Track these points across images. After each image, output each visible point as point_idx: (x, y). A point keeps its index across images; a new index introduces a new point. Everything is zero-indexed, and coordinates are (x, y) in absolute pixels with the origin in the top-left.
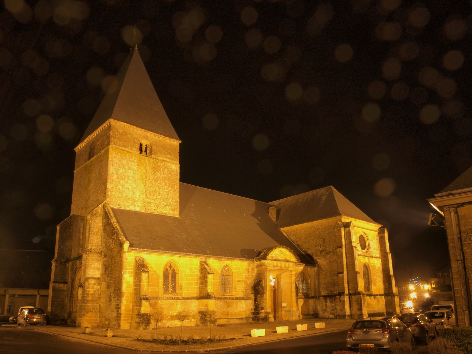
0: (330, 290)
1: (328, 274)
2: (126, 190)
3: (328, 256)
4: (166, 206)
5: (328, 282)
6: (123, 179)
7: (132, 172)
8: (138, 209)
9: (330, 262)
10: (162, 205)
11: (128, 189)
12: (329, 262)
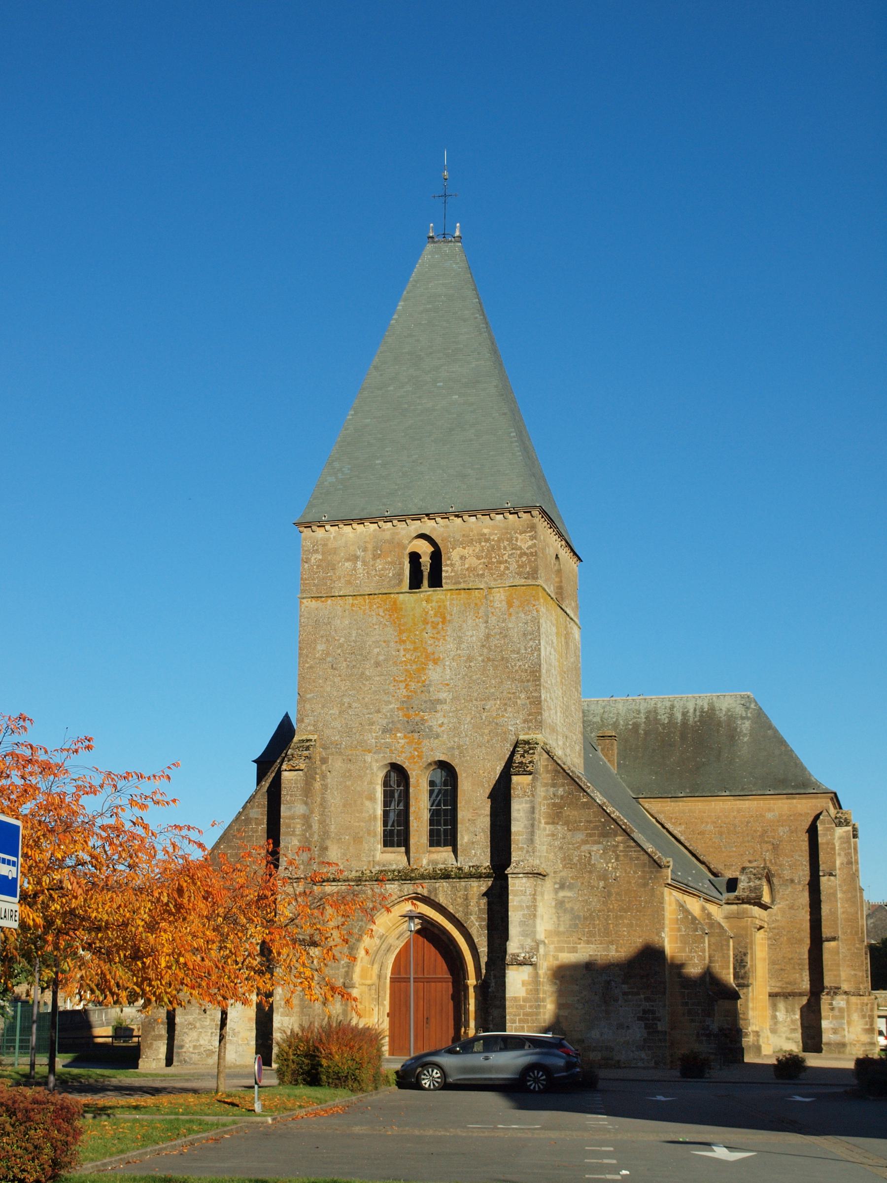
0: (787, 980)
1: (785, 938)
3: (787, 893)
5: (784, 958)
9: (791, 907)
12: (789, 908)
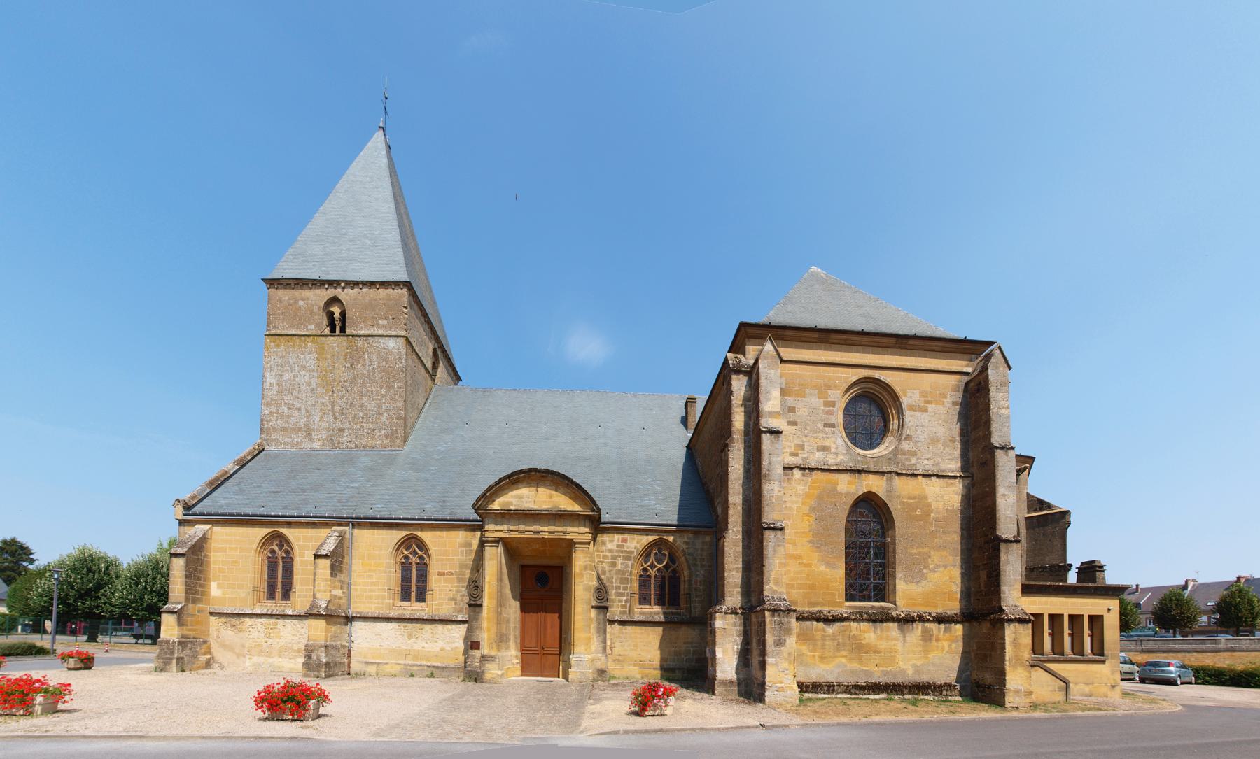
2: (296, 413)
4: (374, 430)
6: (289, 392)
7: (307, 374)
8: (316, 445)
10: (365, 431)
11: (300, 409)
